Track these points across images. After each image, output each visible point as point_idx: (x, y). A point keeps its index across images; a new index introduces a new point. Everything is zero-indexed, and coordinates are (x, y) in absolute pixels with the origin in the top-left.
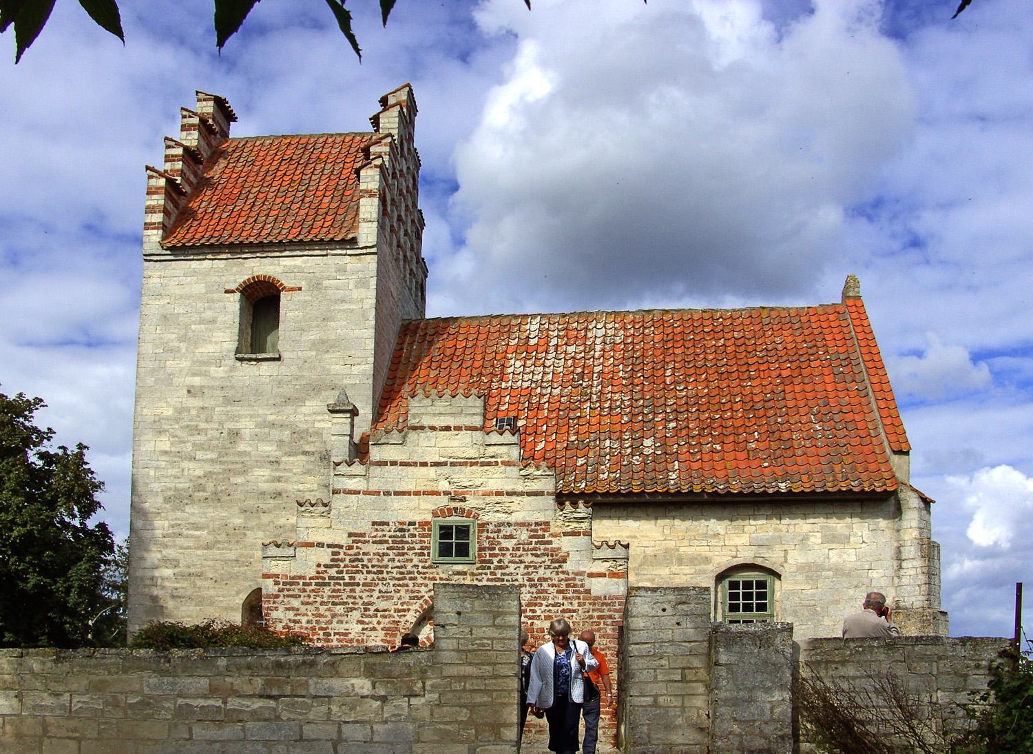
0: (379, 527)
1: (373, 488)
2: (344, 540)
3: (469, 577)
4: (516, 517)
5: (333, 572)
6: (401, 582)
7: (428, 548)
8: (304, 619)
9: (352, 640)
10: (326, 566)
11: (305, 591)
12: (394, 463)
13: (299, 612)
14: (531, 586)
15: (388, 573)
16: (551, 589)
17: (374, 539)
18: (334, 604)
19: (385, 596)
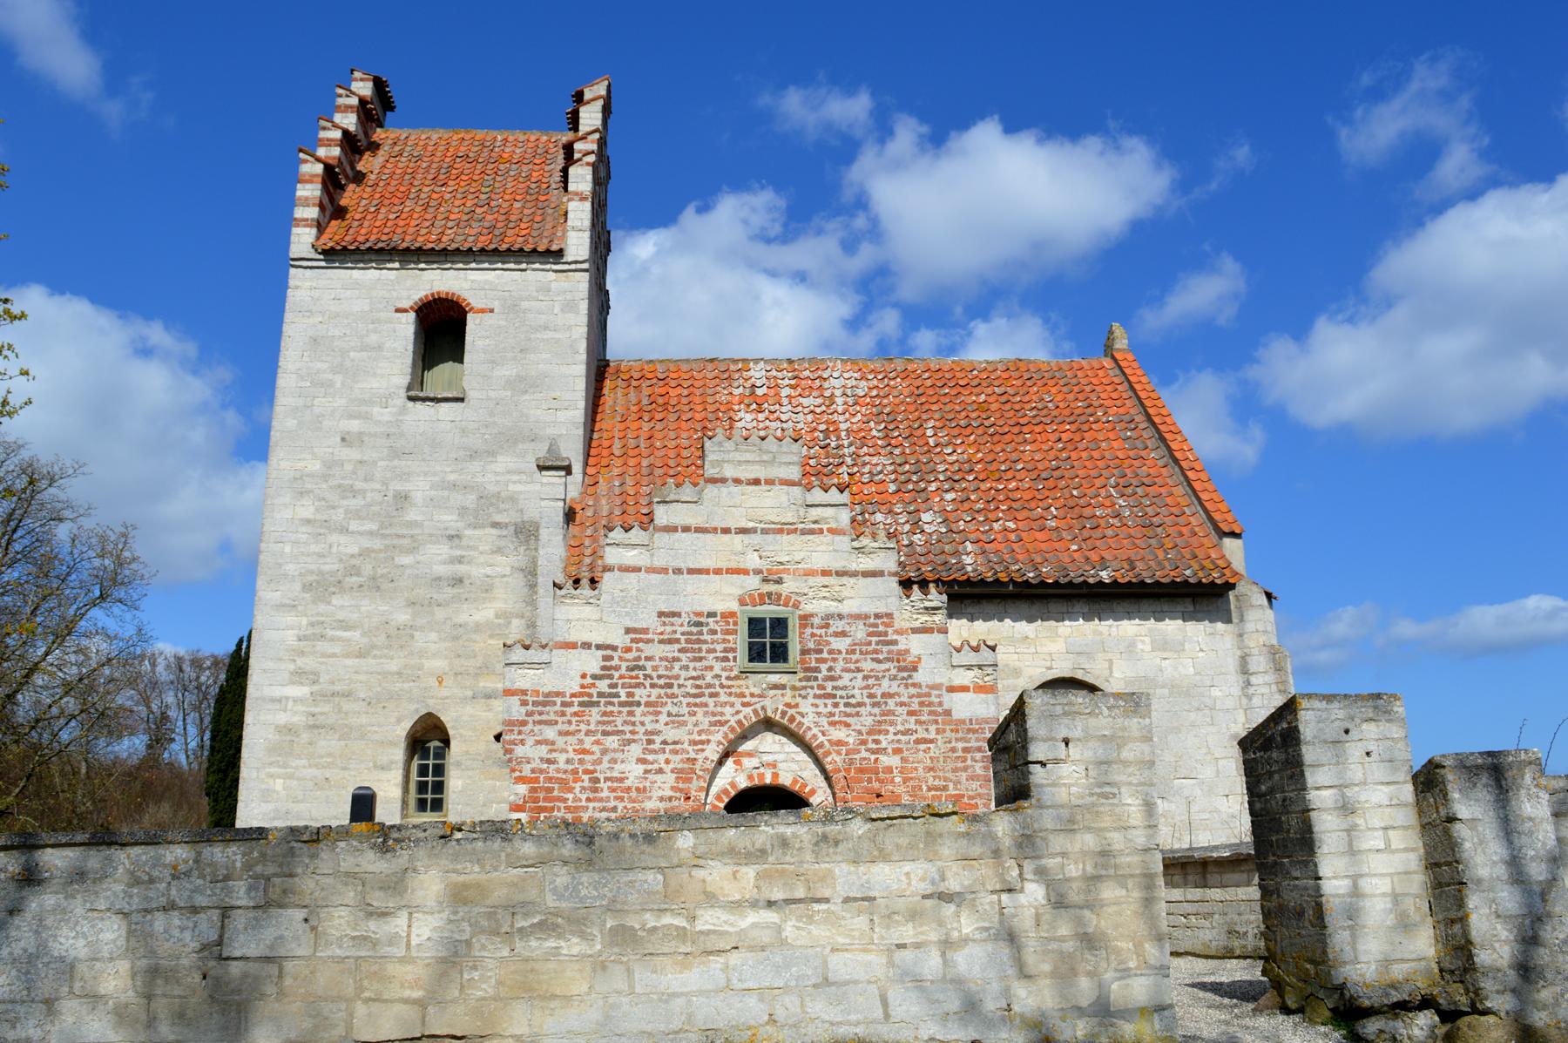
0: (667, 620)
1: (658, 563)
2: (620, 639)
3: (788, 692)
4: (848, 607)
5: (603, 685)
6: (698, 700)
7: (734, 650)
8: (562, 758)
9: (629, 788)
10: (595, 677)
11: (563, 714)
12: (686, 529)
14: (874, 705)
15: (680, 686)
16: (900, 710)
18: (605, 733)
19: (676, 721)
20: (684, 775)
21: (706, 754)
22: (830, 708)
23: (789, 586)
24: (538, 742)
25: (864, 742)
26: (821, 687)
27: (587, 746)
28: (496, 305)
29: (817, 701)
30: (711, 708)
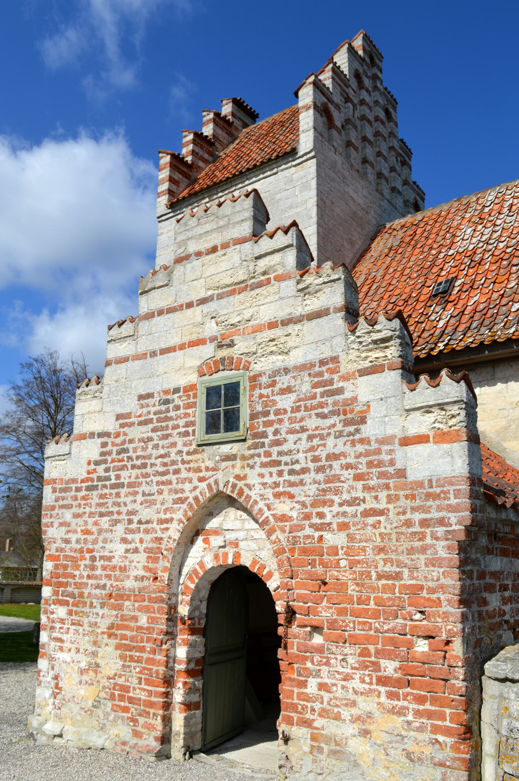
1: (141, 349)
2: (110, 425)
3: (238, 463)
4: (297, 357)
5: (101, 469)
6: (164, 478)
7: (193, 423)
8: (74, 537)
9: (114, 567)
12: (161, 313)
13: (70, 528)
14: (319, 470)
15: (152, 465)
16: (347, 474)
17: (140, 419)
18: (102, 515)
20: (154, 555)
21: (171, 533)
22: (275, 478)
23: (242, 346)
24: (61, 524)
25: (308, 517)
26: (268, 454)
27: (89, 527)
29: (264, 471)
30: (174, 486)
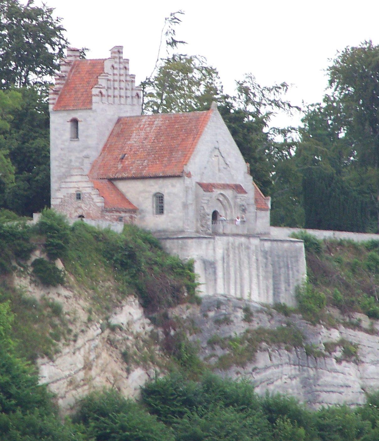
2: (62, 197)
28: (83, 120)
